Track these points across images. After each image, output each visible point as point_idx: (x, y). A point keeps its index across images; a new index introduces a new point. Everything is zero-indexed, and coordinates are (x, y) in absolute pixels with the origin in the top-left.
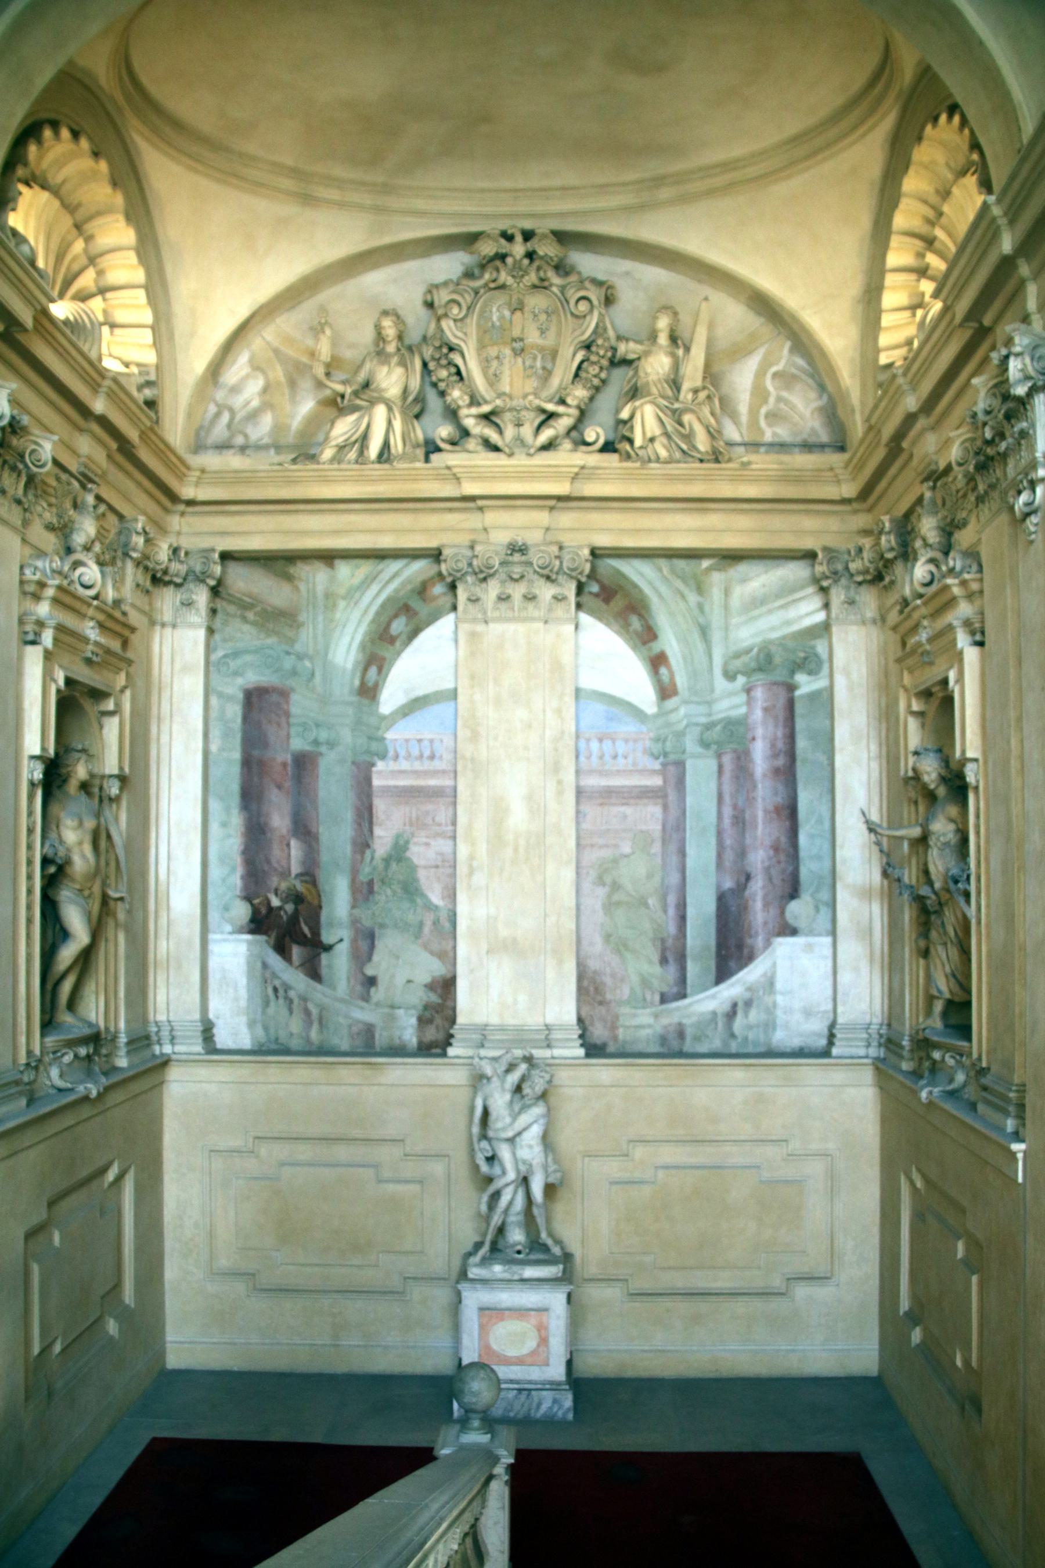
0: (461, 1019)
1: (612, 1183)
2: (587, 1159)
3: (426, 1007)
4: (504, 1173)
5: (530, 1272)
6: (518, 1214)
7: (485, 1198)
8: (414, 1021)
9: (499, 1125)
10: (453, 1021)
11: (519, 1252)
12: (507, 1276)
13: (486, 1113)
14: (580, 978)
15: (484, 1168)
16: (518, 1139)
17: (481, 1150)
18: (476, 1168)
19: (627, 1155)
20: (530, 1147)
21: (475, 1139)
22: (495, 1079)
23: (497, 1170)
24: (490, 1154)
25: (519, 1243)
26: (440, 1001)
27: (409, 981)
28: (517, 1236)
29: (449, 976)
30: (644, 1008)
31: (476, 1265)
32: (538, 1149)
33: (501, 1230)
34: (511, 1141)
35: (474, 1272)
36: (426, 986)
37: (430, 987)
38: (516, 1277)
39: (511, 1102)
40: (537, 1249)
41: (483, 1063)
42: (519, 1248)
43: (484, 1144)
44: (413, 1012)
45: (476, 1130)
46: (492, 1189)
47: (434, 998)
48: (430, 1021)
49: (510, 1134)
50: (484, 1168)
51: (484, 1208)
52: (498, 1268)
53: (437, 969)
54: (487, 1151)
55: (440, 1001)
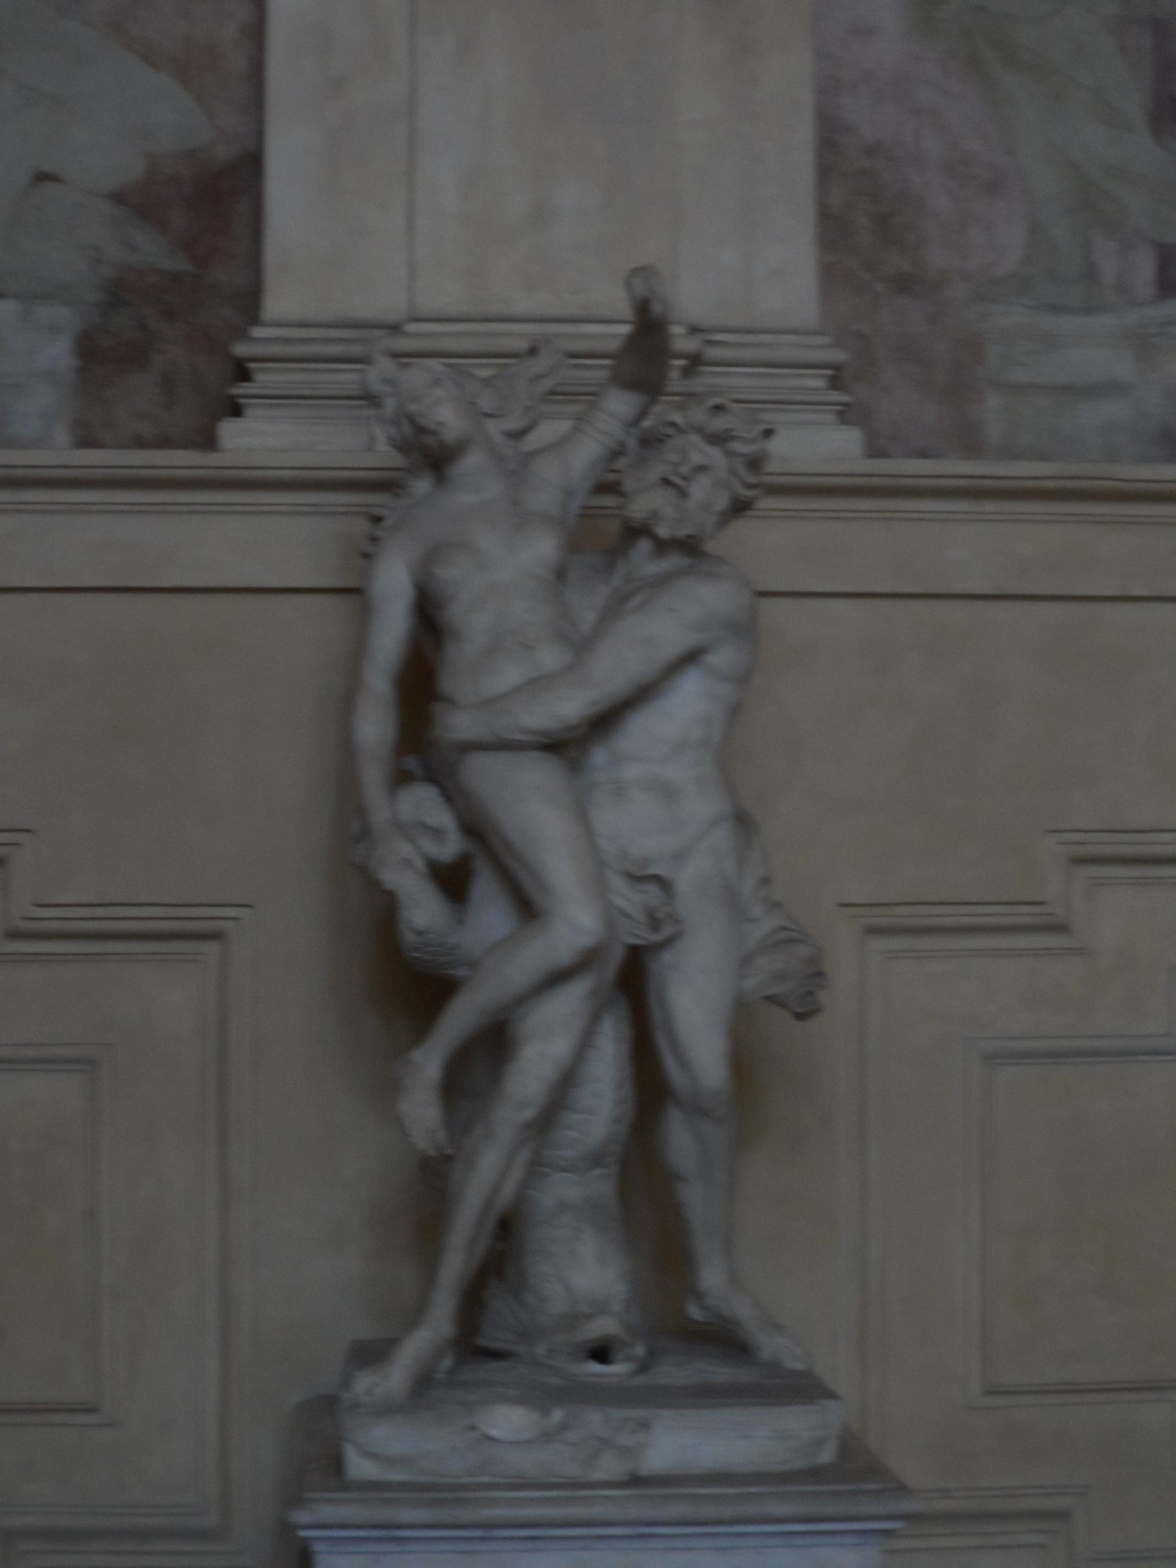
0: (283, 300)
1: (992, 1059)
2: (877, 944)
3: (119, 292)
4: (528, 908)
5: (680, 1442)
6: (595, 1160)
7: (429, 1062)
8: (58, 353)
9: (508, 675)
10: (250, 303)
11: (601, 1353)
12: (558, 1459)
13: (430, 619)
14: (825, 172)
15: (423, 910)
16: (599, 756)
17: (403, 829)
18: (386, 911)
19: (1061, 928)
20: (667, 792)
21: (373, 776)
22: (473, 461)
23: (490, 915)
24: (451, 848)
25: (600, 1308)
26: (182, 265)
27: (43, 177)
28: (583, 1271)
29: (224, 153)
30: (1090, 310)
31: (388, 1410)
32: (703, 806)
33: (507, 1234)
34: (568, 747)
35: (381, 1446)
36: (118, 197)
37: (139, 202)
38: (609, 1467)
39: (561, 574)
40: (691, 1338)
41: (416, 376)
42: (604, 1327)
43: (423, 803)
44: (62, 314)
45: (375, 726)
46: (460, 1018)
47: (153, 251)
48: (135, 355)
49: (569, 706)
50: (423, 910)
51: (421, 1110)
52: (508, 1421)
53: (174, 121)
54: (437, 833)
55: (182, 265)
